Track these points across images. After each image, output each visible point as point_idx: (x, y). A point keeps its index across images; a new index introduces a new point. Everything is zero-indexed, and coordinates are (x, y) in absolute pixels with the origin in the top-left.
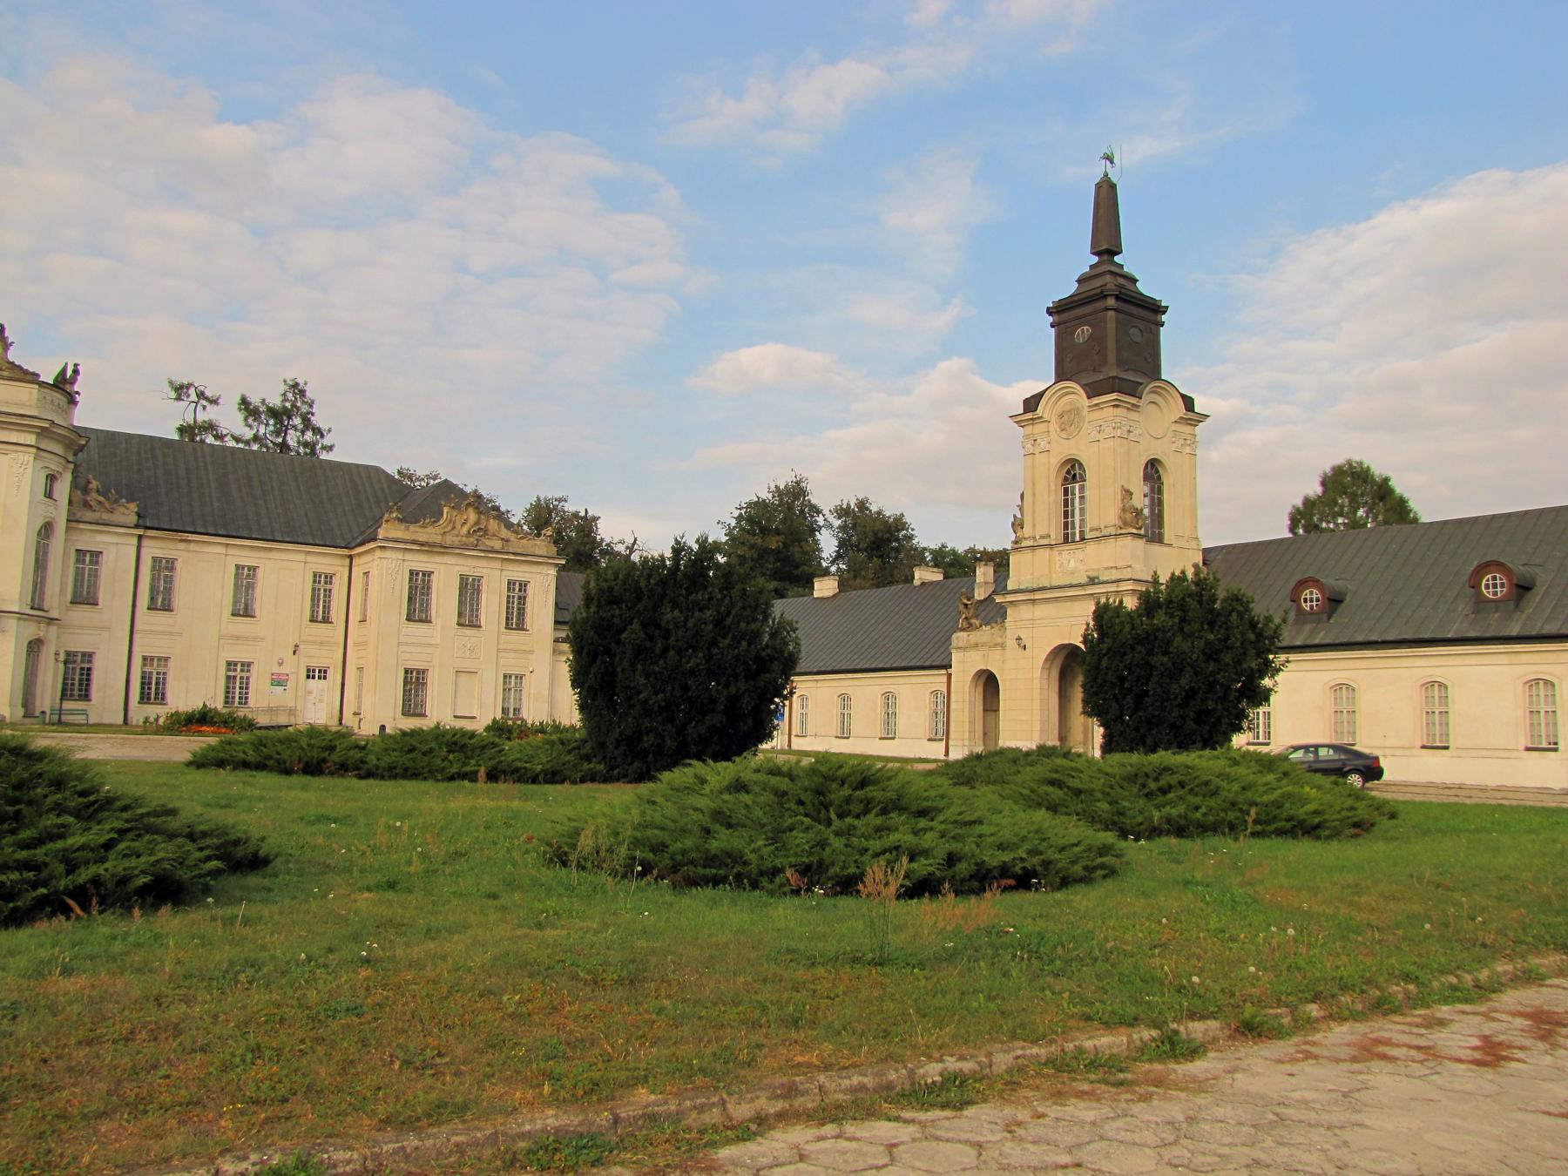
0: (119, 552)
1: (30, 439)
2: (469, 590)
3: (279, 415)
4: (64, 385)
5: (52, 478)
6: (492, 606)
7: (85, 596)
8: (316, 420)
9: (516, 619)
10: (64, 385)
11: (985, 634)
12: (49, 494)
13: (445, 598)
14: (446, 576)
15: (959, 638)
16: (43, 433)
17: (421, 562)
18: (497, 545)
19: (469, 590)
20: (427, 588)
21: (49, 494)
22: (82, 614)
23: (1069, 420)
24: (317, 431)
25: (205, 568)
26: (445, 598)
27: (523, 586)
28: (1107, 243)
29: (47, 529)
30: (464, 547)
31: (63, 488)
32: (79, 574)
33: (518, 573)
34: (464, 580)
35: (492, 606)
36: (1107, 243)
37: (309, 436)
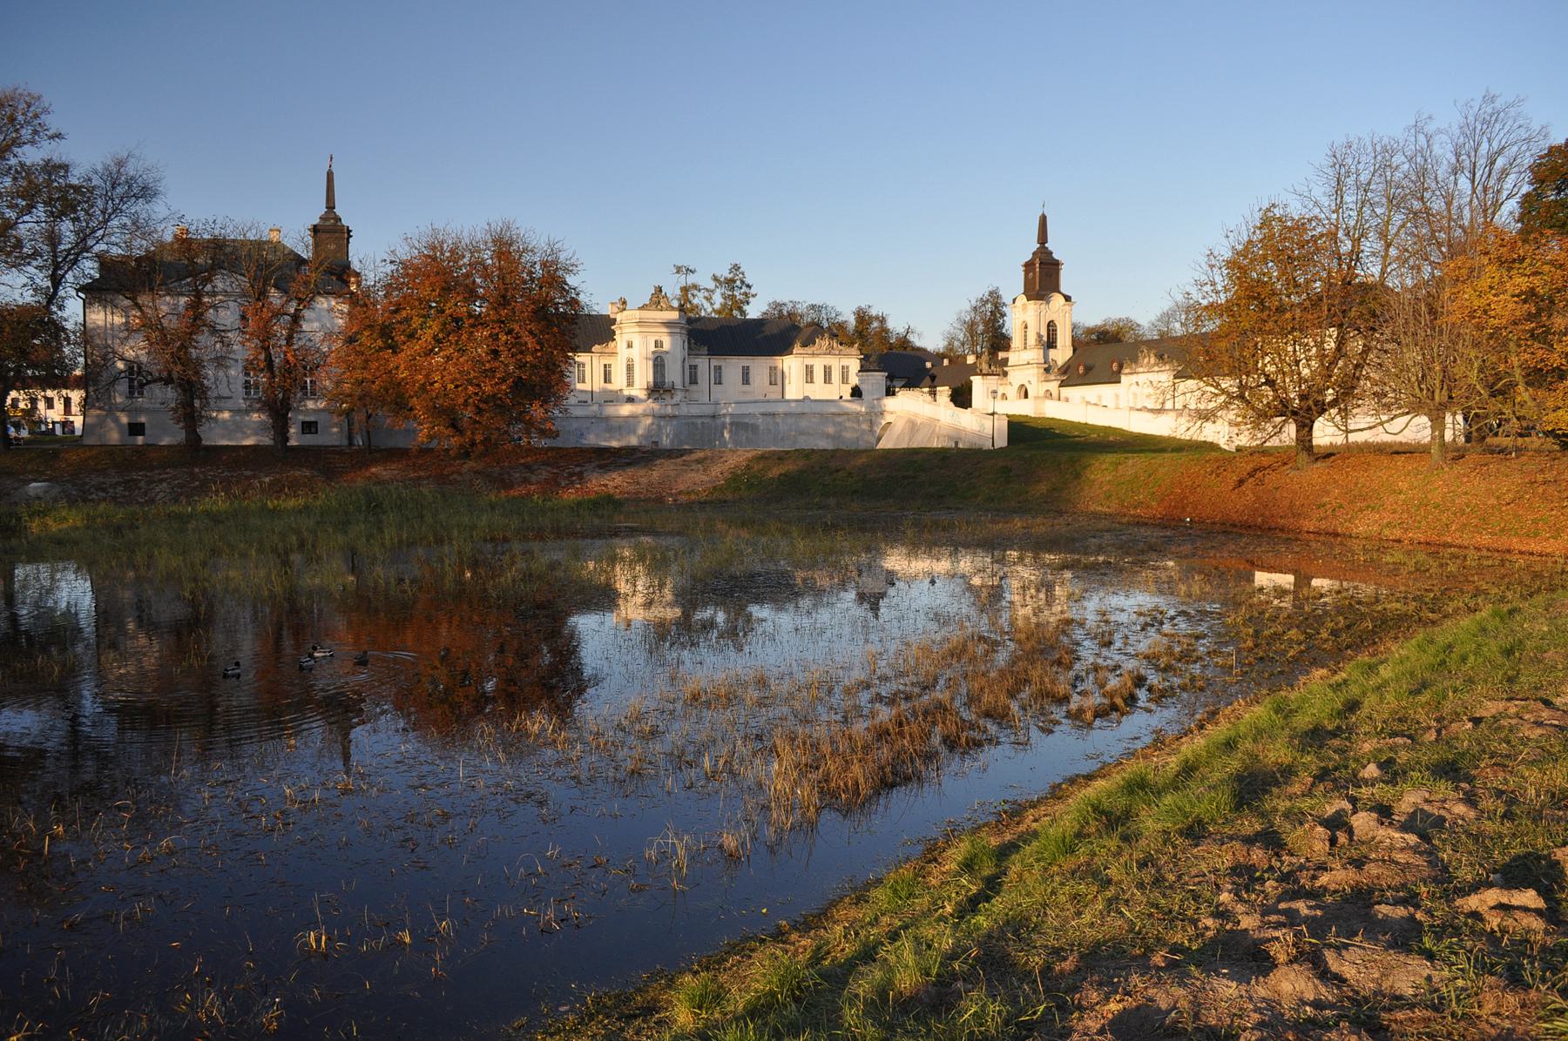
0: (703, 363)
2: (827, 372)
3: (730, 282)
7: (694, 381)
8: (747, 281)
13: (819, 374)
14: (818, 364)
17: (809, 361)
19: (827, 372)
22: (694, 387)
24: (749, 286)
25: (733, 366)
26: (819, 374)
28: (1043, 237)
33: (845, 362)
36: (1043, 237)
37: (744, 289)
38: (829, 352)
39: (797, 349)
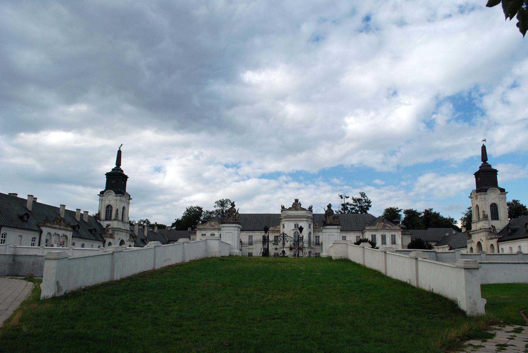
1: (305, 219)
2: (384, 238)
4: (310, 209)
5: (310, 225)
6: (388, 240)
9: (394, 242)
10: (310, 209)
11: (470, 240)
12: (310, 228)
15: (468, 241)
16: (307, 218)
17: (373, 233)
18: (388, 228)
19: (384, 238)
20: (375, 238)
21: (310, 228)
23: (476, 198)
27: (395, 235)
29: (310, 233)
30: (382, 229)
31: (312, 226)
32: (316, 240)
33: (393, 233)
34: (382, 236)
35: (388, 240)
38: (384, 228)
39: (367, 228)
